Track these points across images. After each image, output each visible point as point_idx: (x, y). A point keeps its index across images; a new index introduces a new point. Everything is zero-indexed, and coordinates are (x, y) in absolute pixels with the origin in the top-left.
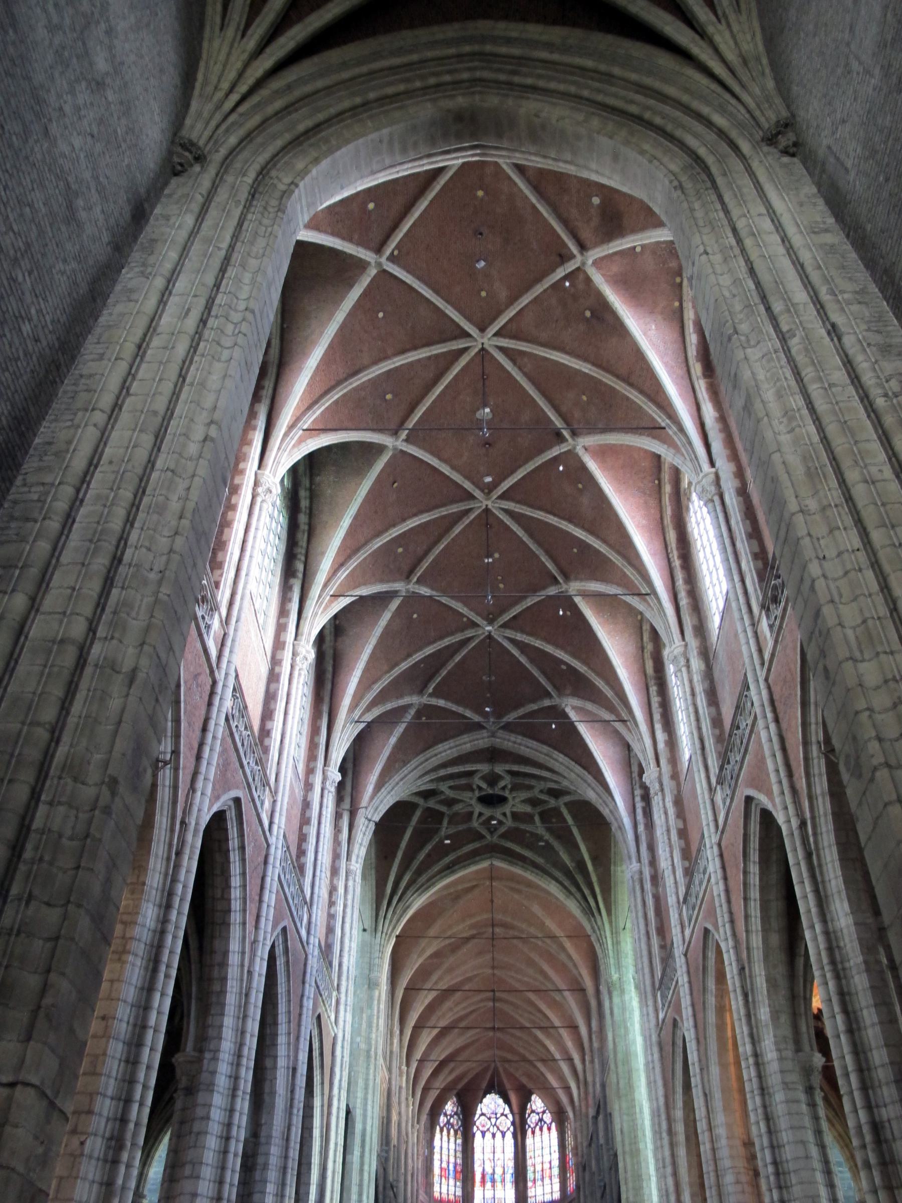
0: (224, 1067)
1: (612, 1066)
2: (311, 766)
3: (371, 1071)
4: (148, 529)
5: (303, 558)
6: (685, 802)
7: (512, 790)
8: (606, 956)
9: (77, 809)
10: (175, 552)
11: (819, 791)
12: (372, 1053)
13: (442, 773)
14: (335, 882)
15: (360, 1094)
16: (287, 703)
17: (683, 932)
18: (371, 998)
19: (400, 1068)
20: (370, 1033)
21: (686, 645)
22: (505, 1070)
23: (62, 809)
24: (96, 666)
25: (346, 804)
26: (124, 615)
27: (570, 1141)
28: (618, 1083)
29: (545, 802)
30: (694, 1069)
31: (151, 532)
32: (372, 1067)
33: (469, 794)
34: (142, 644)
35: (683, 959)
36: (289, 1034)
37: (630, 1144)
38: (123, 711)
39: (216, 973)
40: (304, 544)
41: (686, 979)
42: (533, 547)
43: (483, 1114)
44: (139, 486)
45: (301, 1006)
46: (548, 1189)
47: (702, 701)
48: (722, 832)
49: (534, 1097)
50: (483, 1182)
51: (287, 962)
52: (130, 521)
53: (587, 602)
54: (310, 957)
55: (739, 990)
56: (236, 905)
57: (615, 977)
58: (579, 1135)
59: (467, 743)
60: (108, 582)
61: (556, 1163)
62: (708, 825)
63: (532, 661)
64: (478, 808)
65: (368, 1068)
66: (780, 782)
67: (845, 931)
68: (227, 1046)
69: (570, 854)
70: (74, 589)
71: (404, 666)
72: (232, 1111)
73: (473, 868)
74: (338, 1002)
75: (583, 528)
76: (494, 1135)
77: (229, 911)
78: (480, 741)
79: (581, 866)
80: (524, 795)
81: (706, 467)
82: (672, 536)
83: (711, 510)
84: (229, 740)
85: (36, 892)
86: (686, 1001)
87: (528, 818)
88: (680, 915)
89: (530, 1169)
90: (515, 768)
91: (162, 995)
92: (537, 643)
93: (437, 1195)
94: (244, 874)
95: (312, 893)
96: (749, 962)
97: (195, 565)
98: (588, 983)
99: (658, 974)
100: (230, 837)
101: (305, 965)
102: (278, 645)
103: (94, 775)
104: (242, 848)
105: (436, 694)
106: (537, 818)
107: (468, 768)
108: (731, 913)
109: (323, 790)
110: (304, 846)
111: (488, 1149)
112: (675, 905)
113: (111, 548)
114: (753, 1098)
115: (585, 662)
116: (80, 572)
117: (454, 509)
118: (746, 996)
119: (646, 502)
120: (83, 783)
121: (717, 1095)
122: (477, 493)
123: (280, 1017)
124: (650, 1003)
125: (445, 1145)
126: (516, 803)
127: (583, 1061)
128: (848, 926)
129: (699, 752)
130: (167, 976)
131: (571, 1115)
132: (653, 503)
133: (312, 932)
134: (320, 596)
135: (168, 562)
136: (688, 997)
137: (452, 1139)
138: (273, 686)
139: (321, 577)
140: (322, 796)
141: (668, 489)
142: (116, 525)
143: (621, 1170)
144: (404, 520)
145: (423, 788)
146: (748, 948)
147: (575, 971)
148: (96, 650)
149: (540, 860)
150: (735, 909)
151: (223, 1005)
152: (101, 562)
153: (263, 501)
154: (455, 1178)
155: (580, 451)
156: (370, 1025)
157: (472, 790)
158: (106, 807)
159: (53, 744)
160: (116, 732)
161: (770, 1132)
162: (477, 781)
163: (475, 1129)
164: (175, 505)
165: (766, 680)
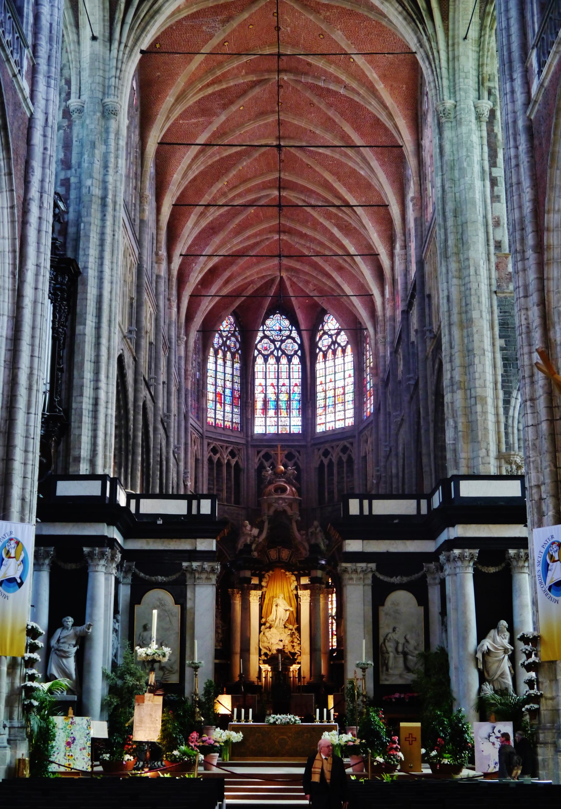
3: (109, 223)
8: (437, 76)
12: (109, 200)
15: (94, 251)
19: (157, 254)
22: (293, 284)
27: (369, 360)
28: (446, 240)
37: (460, 313)
43: (265, 337)
49: (326, 318)
50: (265, 409)
57: (449, 103)
58: (381, 348)
61: (350, 388)
65: (103, 220)
74: (34, 71)
76: (278, 360)
89: (320, 396)
124: (518, 75)
127: (392, 256)
131: (371, 330)
137: (229, 363)
154: (232, 404)
163: (256, 353)
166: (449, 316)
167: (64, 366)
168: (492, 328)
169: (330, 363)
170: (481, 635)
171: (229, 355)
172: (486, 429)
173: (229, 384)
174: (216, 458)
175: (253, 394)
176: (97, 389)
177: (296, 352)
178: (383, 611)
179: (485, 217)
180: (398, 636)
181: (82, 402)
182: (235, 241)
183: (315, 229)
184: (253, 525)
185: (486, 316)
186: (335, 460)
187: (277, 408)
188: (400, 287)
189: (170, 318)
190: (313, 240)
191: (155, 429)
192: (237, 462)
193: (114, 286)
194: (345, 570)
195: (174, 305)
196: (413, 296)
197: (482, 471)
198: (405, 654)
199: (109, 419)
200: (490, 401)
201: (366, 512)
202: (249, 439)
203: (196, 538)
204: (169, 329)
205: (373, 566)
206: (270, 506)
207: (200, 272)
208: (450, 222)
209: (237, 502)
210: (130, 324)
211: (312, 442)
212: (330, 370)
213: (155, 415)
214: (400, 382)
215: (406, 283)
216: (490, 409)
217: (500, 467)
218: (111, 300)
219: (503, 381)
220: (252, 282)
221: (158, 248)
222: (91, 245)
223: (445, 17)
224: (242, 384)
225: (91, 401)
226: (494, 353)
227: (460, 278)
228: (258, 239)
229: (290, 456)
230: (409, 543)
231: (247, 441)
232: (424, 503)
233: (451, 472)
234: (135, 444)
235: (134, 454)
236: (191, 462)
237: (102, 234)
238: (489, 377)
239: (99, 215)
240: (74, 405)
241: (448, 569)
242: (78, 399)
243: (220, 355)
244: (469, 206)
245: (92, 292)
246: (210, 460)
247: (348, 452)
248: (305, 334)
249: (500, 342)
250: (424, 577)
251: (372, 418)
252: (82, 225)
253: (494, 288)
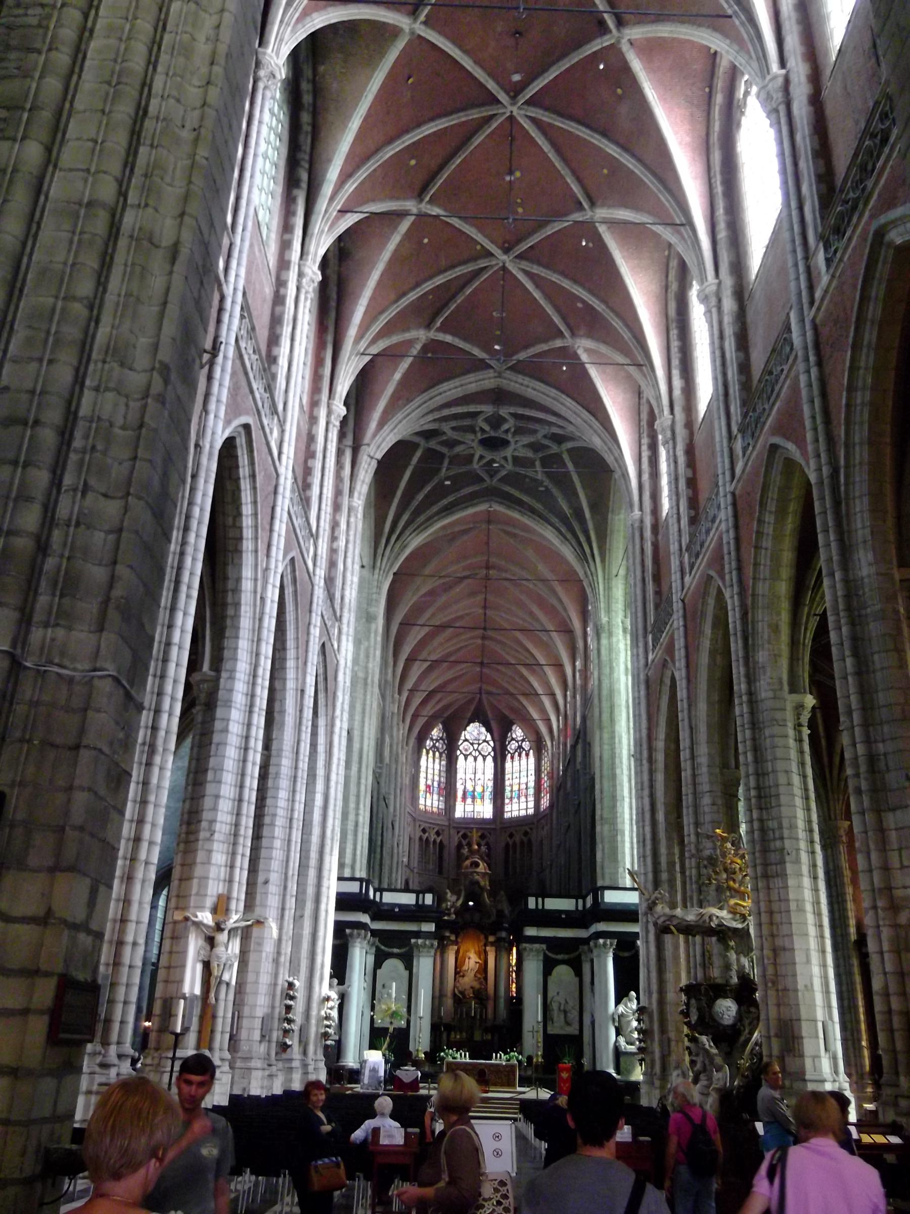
0: (240, 687)
1: (596, 701)
2: (316, 398)
3: (368, 697)
4: (175, 75)
5: (307, 166)
6: (697, 453)
7: (515, 433)
8: (597, 600)
9: (127, 396)
10: (209, 106)
11: (857, 440)
13: (446, 412)
14: (338, 518)
16: (294, 328)
17: (682, 578)
18: (369, 630)
20: (368, 662)
21: (719, 284)
23: (110, 395)
24: (131, 237)
25: (349, 441)
26: (158, 180)
29: (548, 447)
30: (683, 705)
31: (179, 79)
32: (369, 694)
33: (472, 437)
34: (182, 214)
35: (680, 604)
36: (298, 658)
38: (168, 289)
39: (230, 599)
40: (308, 149)
41: (681, 623)
42: (558, 164)
43: (466, 740)
44: (158, 20)
45: (308, 634)
46: (523, 806)
47: (730, 345)
48: (738, 481)
50: (464, 798)
51: (295, 592)
52: (152, 63)
53: (612, 233)
54: (316, 588)
55: (739, 634)
56: (248, 533)
57: (604, 619)
59: (472, 383)
60: (135, 135)
61: (532, 784)
62: (724, 473)
63: (548, 297)
64: (479, 451)
65: (365, 695)
66: (815, 429)
67: (866, 580)
68: (243, 666)
69: (569, 502)
70: (95, 142)
71: (413, 296)
72: (249, 725)
73: (471, 511)
75: (617, 143)
76: (475, 759)
77: (241, 538)
78: (486, 382)
79: (579, 514)
80: (526, 440)
81: (775, 67)
82: (717, 157)
83: (774, 121)
84: (238, 362)
85: (92, 482)
86: (680, 643)
87: (529, 463)
88: (681, 563)
89: (508, 789)
90: (520, 411)
91: (185, 614)
92: (555, 278)
93: (422, 807)
94: (255, 502)
95: (318, 526)
96: (753, 608)
97: (230, 127)
98: (577, 624)
99: (651, 618)
100: (241, 464)
101: (312, 595)
102: (283, 264)
103: (142, 360)
104: (253, 476)
105: (443, 329)
106: (538, 463)
107: (472, 408)
108: (739, 560)
109: (328, 423)
110: (309, 479)
111: (470, 770)
112: (677, 553)
113: (135, 94)
114: (743, 731)
115: (604, 301)
116: (101, 122)
117: (475, 114)
118: (745, 639)
119: (692, 115)
120: (131, 369)
121: (703, 729)
122: (502, 97)
123: (288, 643)
124: (641, 644)
125: (430, 765)
126: (518, 447)
127: (565, 696)
128: (869, 576)
129: (721, 398)
130: (188, 596)
131: (549, 743)
132: (700, 115)
133: (318, 563)
134: (326, 211)
135: (202, 118)
136: (682, 640)
137: (437, 761)
138: (278, 309)
139: (327, 189)
140: (327, 430)
141: (719, 99)
142: (137, 63)
143: (597, 792)
144: (419, 125)
145: (426, 427)
146: (753, 595)
147: (564, 614)
148: (129, 219)
149: (538, 506)
150: (744, 555)
151: (237, 628)
152: (124, 110)
153: (265, 88)
154: (439, 794)
155: (625, 47)
156: (367, 657)
157: (474, 432)
158: (159, 395)
159: (93, 324)
160: (162, 314)
161: (756, 761)
162: (481, 423)
164: (203, 48)
165: (813, 321)
169: (516, 763)
170: (618, 1002)
174: (425, 836)
176: (357, 815)
178: (551, 980)
180: (560, 999)
184: (453, 892)
185: (626, 772)
187: (473, 798)
194: (525, 949)
198: (565, 1012)
201: (540, 907)
205: (544, 946)
212: (516, 768)
223: (603, 560)
229: (483, 837)
232: (580, 902)
233: (600, 883)
241: (595, 952)
246: (421, 839)
250: (579, 956)
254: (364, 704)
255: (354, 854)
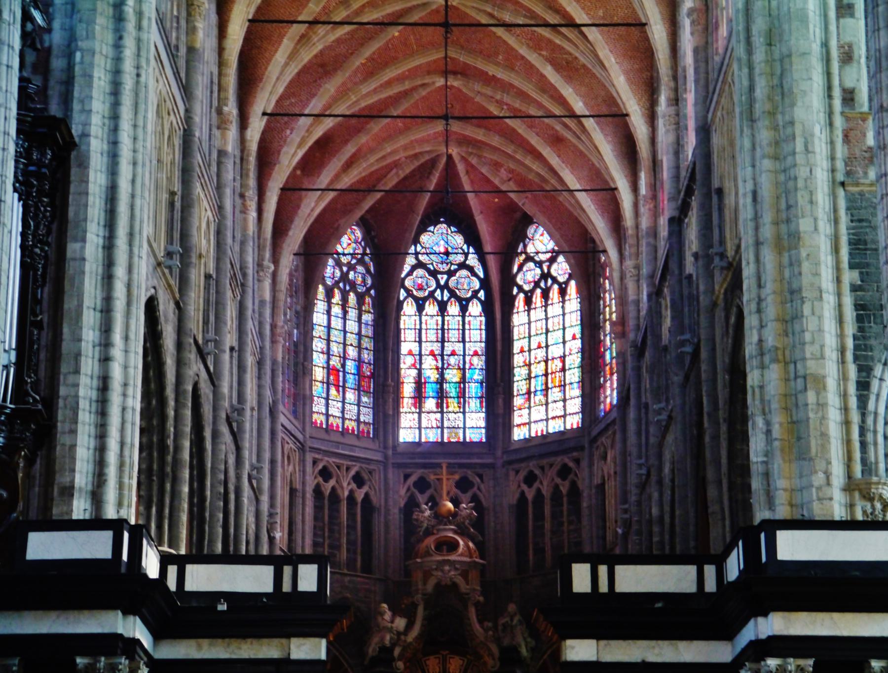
15: (99, 105)
19: (219, 112)
22: (471, 169)
27: (610, 309)
28: (751, 88)
37: (776, 223)
43: (420, 265)
49: (530, 231)
50: (419, 397)
58: (631, 285)
61: (574, 360)
76: (443, 307)
89: (520, 373)
127: (652, 118)
131: (613, 254)
137: (352, 314)
154: (359, 389)
163: (403, 294)
166: (757, 229)
167: (44, 318)
168: (836, 250)
169: (537, 314)
171: (352, 298)
172: (824, 436)
173: (352, 352)
174: (327, 487)
175: (398, 369)
176: (105, 360)
177: (475, 294)
179: (825, 45)
181: (77, 385)
182: (365, 89)
183: (511, 68)
185: (825, 228)
186: (546, 491)
187: (441, 396)
188: (666, 174)
189: (245, 229)
190: (506, 87)
191: (215, 435)
192: (367, 495)
193: (139, 169)
195: (252, 205)
196: (689, 192)
197: (818, 512)
199: (129, 416)
200: (831, 383)
201: (604, 588)
202: (390, 452)
203: (289, 636)
204: (242, 251)
206: (427, 575)
207: (300, 146)
208: (759, 56)
209: (367, 568)
210: (170, 240)
211: (505, 458)
213: (215, 409)
214: (666, 349)
215: (678, 167)
216: (833, 399)
217: (852, 506)
218: (133, 196)
219: (856, 348)
220: (396, 165)
221: (222, 101)
222: (95, 93)
224: (376, 351)
225: (95, 383)
226: (839, 295)
227: (776, 158)
228: (407, 85)
229: (464, 485)
230: (682, 645)
231: (386, 457)
232: (710, 571)
233: (761, 514)
234: (176, 462)
235: (175, 480)
236: (282, 495)
237: (117, 72)
238: (830, 341)
239: (110, 38)
240: (63, 391)
242: (71, 379)
243: (337, 298)
244: (795, 24)
245: (97, 180)
246: (318, 492)
247: (571, 476)
248: (491, 260)
249: (850, 277)
251: (614, 414)
252: (78, 55)
253: (840, 177)
254: (117, 72)
255: (100, 464)
